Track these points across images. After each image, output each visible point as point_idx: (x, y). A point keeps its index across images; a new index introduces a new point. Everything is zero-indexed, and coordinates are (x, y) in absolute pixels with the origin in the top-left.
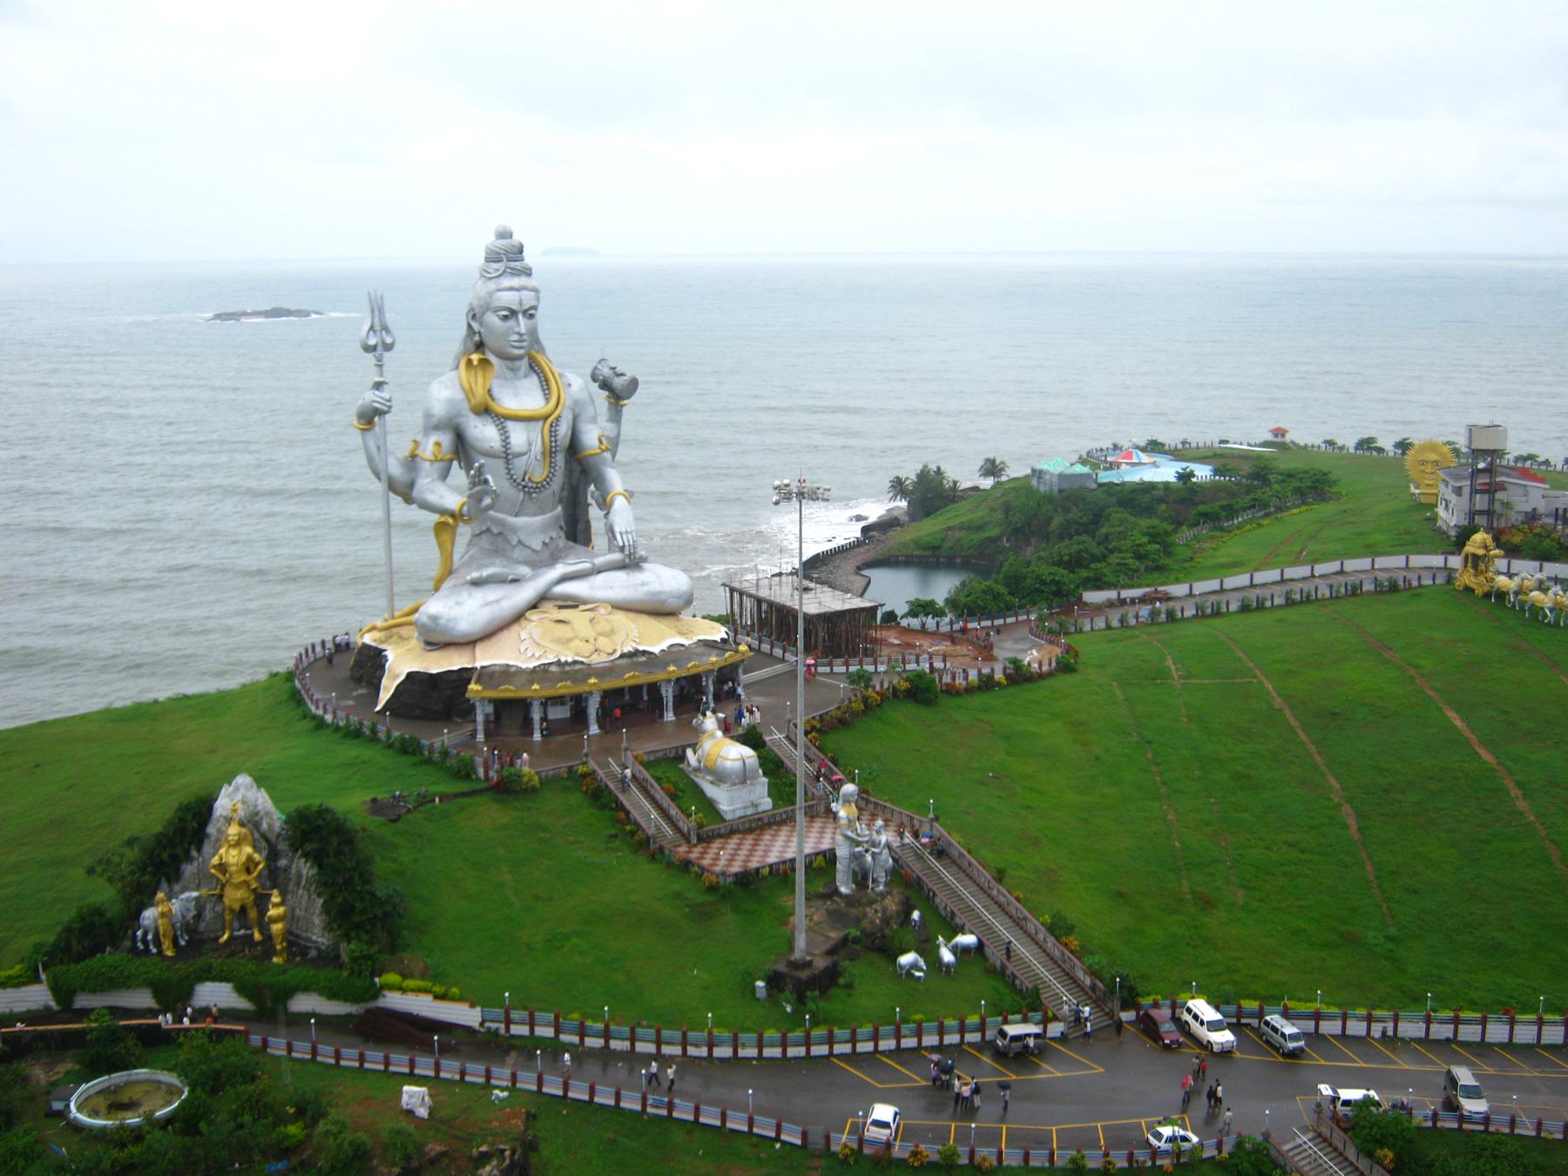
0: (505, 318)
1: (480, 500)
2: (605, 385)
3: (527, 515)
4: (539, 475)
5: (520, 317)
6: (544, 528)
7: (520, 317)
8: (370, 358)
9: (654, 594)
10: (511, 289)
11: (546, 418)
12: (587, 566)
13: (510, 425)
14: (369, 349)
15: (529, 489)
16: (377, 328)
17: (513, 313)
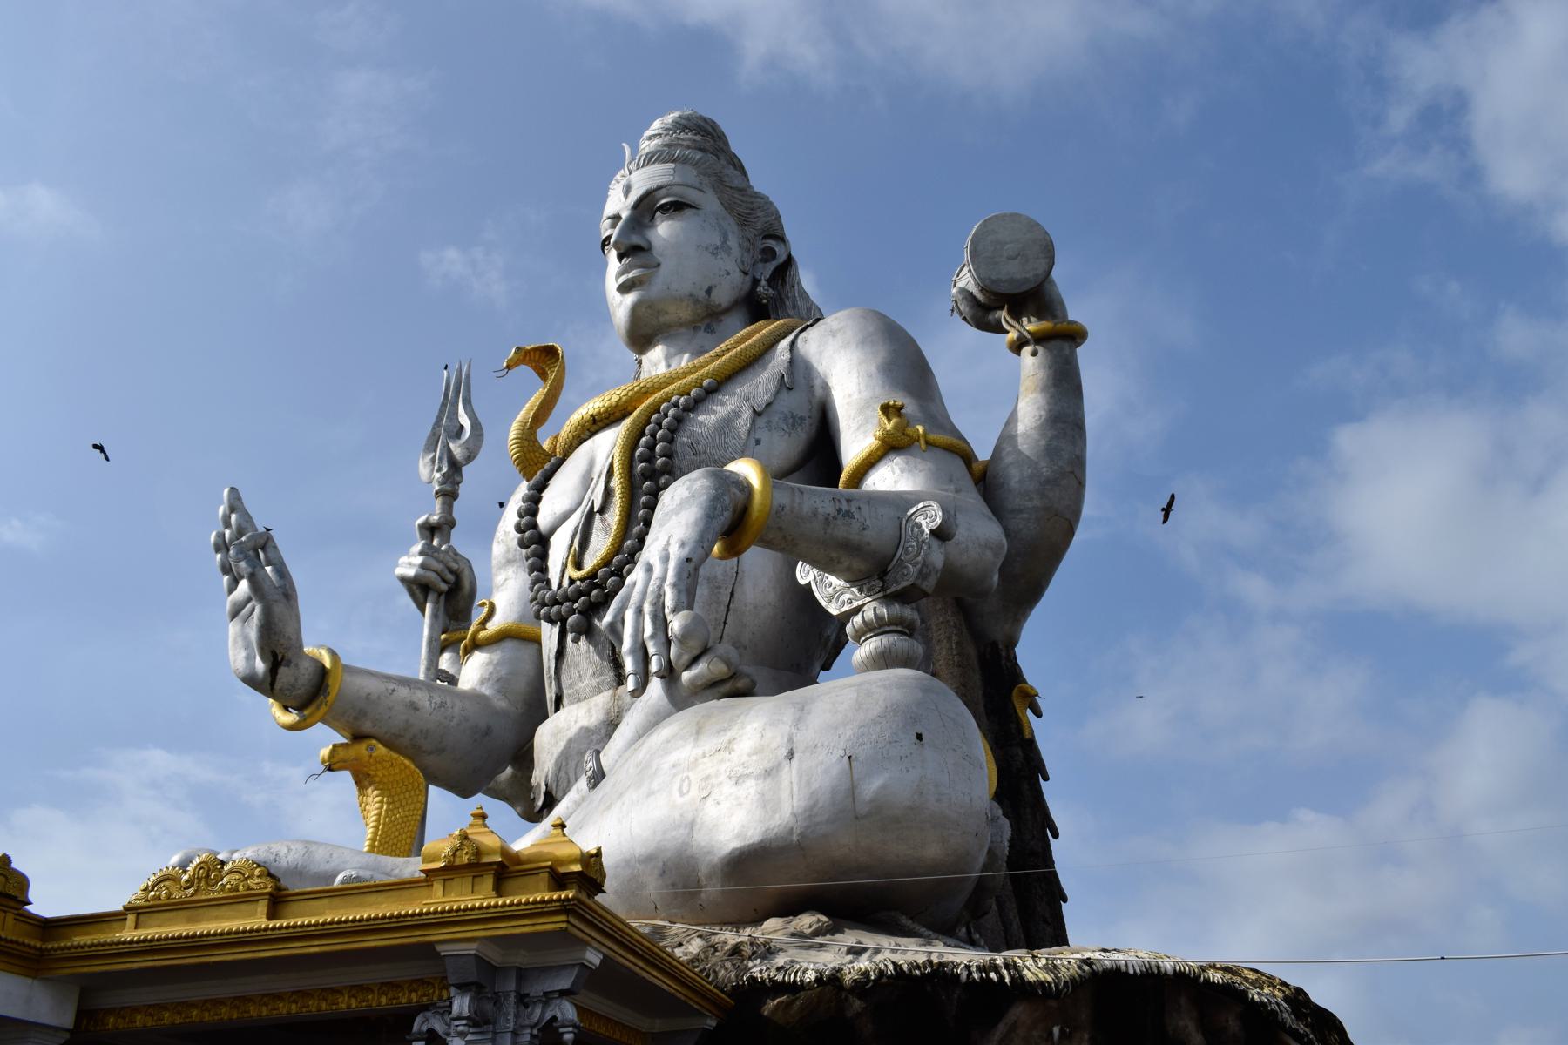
3: (578, 699)
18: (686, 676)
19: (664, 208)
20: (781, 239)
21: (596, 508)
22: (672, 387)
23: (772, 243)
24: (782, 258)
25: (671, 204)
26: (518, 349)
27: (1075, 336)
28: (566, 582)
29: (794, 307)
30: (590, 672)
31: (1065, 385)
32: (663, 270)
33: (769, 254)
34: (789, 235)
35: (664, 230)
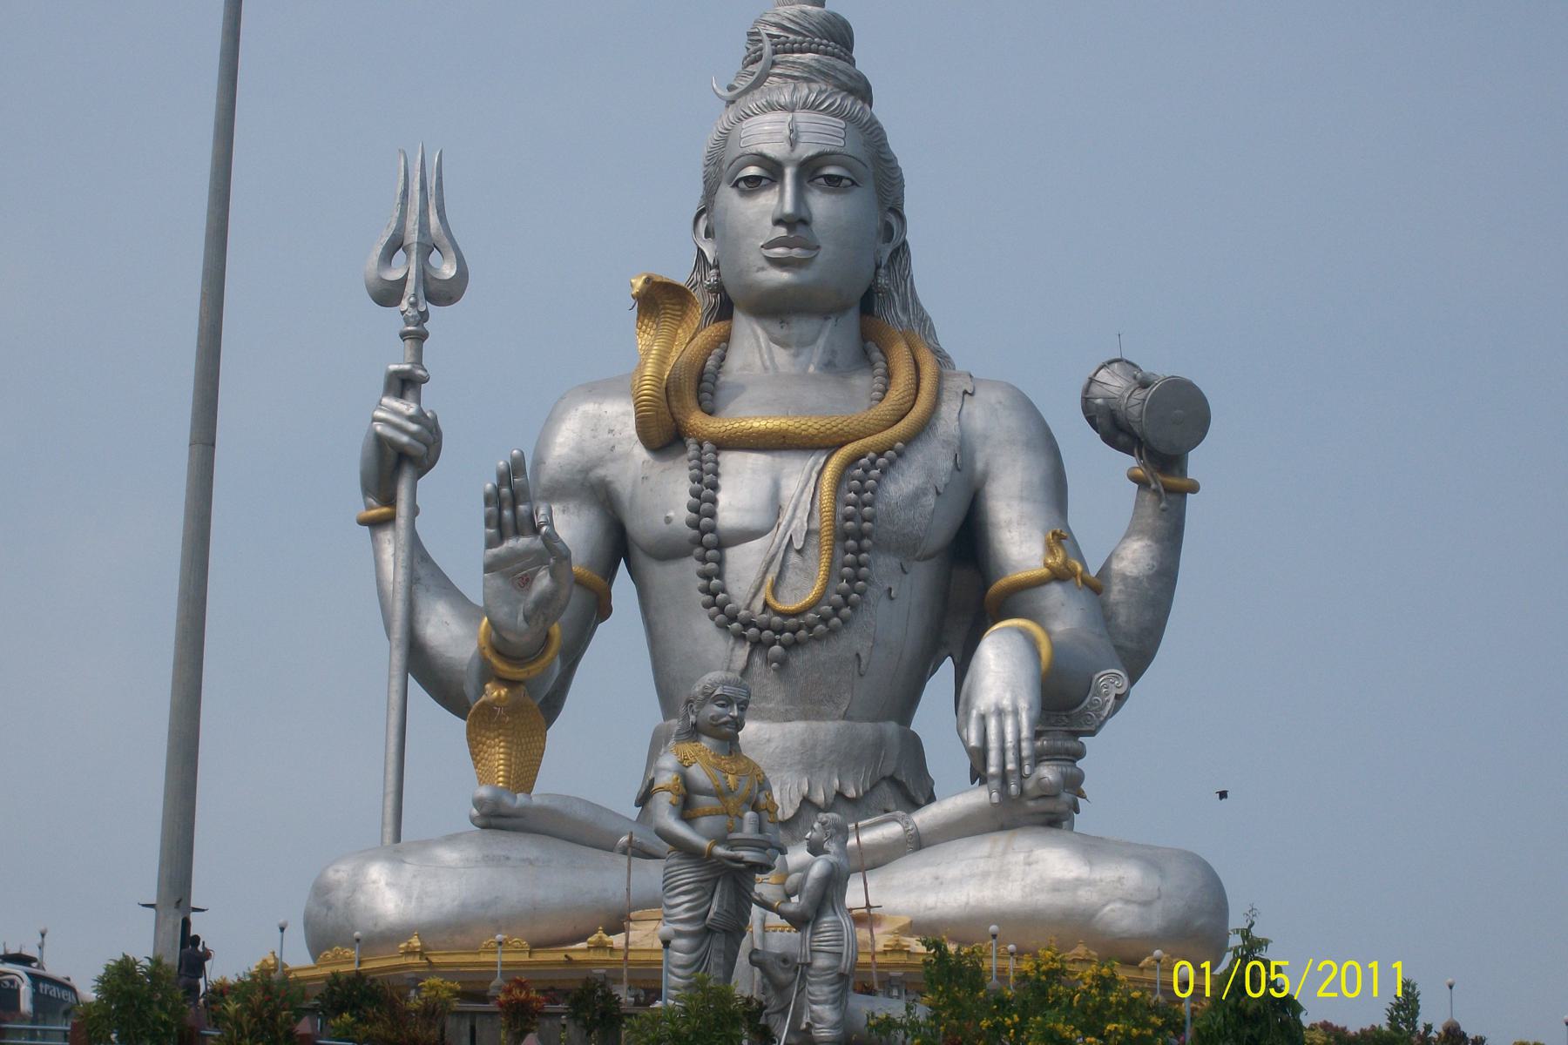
0: (752, 186)
1: (526, 582)
2: (1112, 426)
3: (762, 716)
4: (802, 591)
5: (789, 173)
6: (809, 761)
7: (789, 173)
8: (392, 319)
9: (1057, 886)
10: (771, 107)
11: (841, 445)
12: (892, 830)
13: (731, 461)
14: (387, 295)
15: (773, 638)
16: (412, 237)
17: (772, 171)
18: (1031, 804)
19: (833, 181)
20: (901, 218)
21: (798, 545)
22: (869, 440)
23: (893, 220)
24: (896, 242)
25: (840, 178)
26: (648, 280)
27: (1194, 488)
28: (758, 605)
29: (905, 309)
30: (779, 697)
31: (1170, 538)
32: (822, 252)
33: (888, 233)
34: (908, 210)
35: (821, 204)
